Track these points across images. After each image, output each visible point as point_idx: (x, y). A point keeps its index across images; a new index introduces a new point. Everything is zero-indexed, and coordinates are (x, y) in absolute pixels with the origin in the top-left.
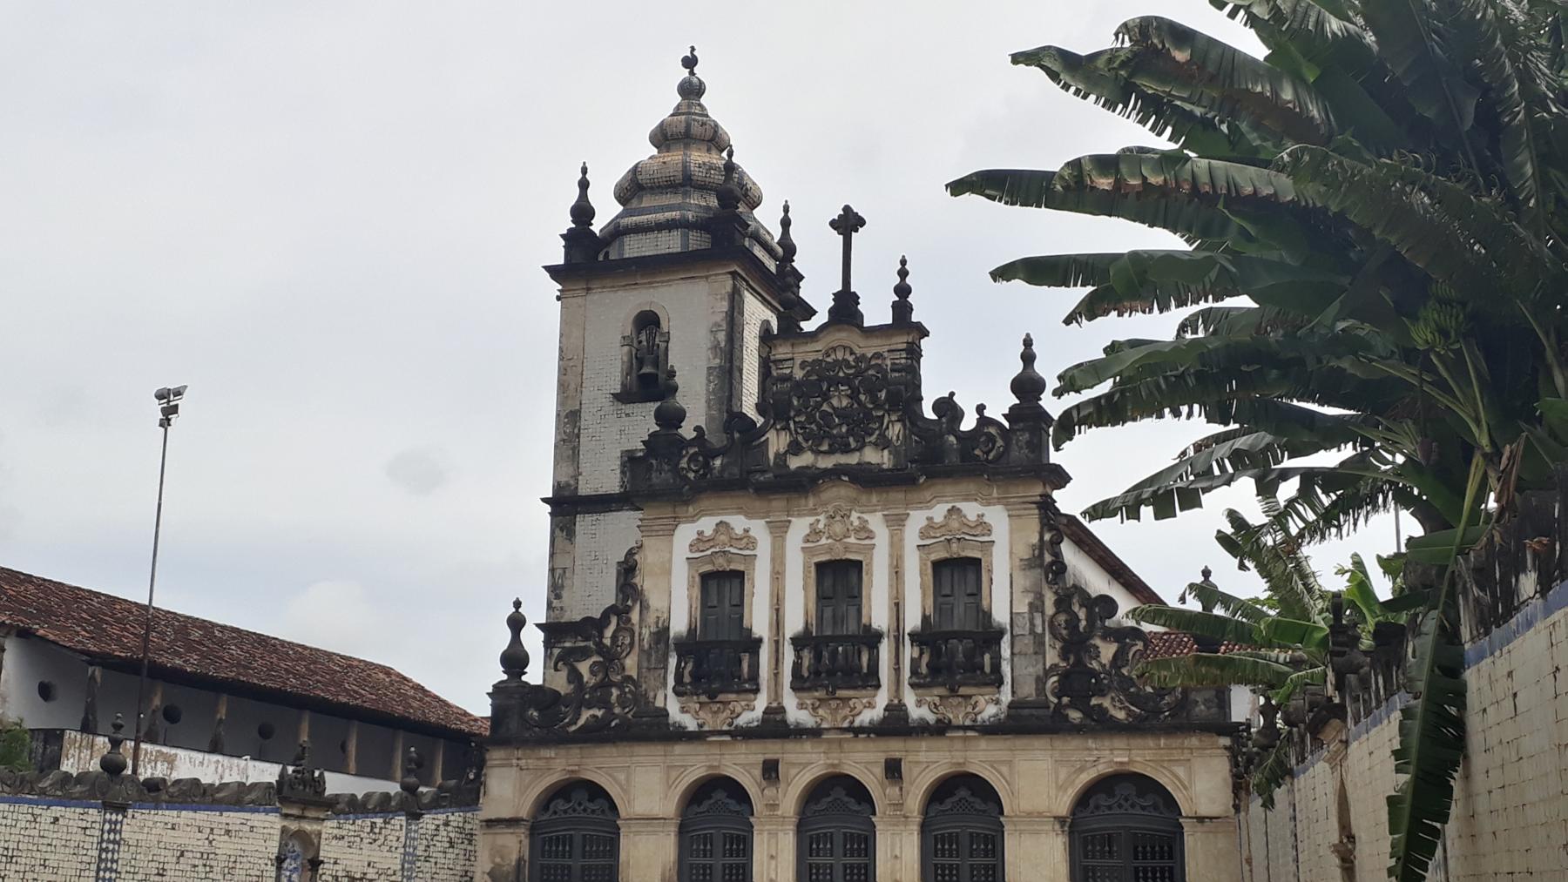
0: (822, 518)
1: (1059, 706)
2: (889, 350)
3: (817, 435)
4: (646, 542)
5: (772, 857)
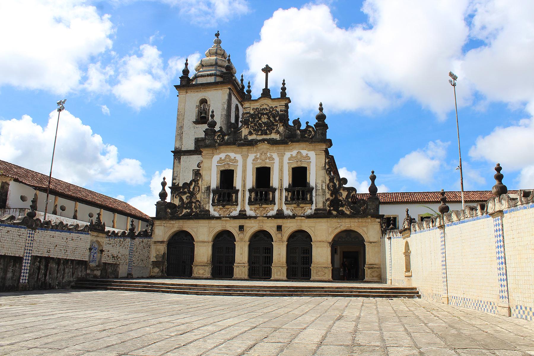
0: (258, 154)
1: (330, 210)
2: (279, 106)
3: (258, 129)
4: (204, 160)
5: (241, 254)
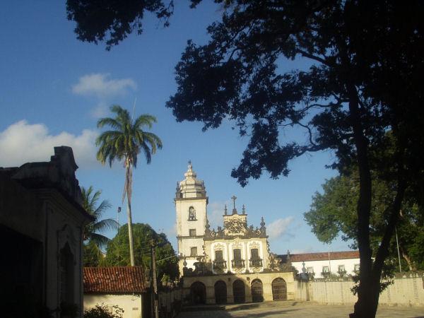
2: (243, 218)
